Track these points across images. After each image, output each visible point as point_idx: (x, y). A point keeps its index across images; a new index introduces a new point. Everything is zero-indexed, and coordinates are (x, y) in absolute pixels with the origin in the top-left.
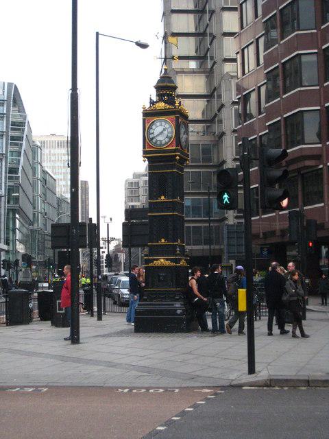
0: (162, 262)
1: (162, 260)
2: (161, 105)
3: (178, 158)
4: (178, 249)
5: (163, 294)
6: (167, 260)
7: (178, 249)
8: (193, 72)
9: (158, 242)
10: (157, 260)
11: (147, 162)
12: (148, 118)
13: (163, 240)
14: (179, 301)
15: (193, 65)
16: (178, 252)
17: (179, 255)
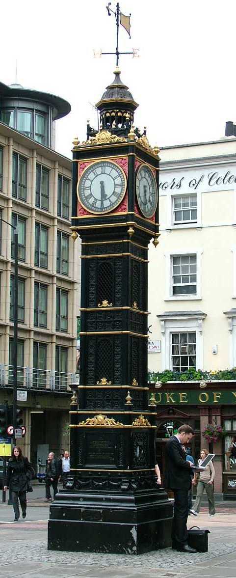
0: (101, 420)
1: (100, 417)
2: (105, 137)
3: (131, 230)
4: (129, 397)
5: (99, 480)
6: (109, 416)
7: (129, 397)
9: (96, 384)
10: (92, 416)
13: (104, 380)
16: (129, 403)
17: (129, 408)
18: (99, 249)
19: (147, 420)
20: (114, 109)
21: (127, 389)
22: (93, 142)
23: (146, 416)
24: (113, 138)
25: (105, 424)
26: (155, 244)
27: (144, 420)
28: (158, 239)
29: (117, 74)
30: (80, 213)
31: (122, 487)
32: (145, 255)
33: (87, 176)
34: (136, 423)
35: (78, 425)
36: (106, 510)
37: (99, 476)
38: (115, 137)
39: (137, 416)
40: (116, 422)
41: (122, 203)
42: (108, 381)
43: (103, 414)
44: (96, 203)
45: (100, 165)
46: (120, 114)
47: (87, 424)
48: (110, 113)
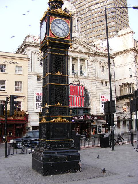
0: (59, 119)
5: (61, 144)
6: (63, 118)
9: (55, 105)
10: (56, 118)
12: (51, 17)
13: (58, 104)
18: (57, 51)
36: (68, 157)
37: (61, 143)
41: (68, 36)
42: (60, 104)
43: (60, 117)
48: (58, 4)
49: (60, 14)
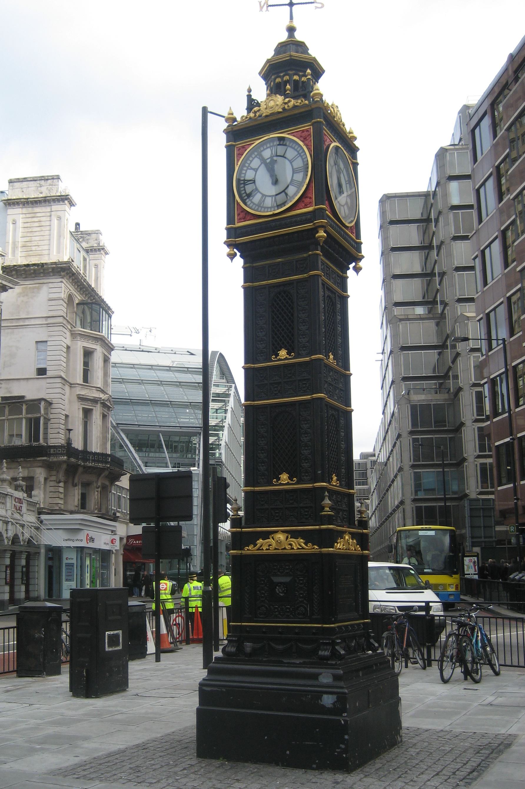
3: (322, 233)
4: (327, 501)
6: (295, 535)
7: (327, 501)
8: (420, 318)
10: (266, 535)
11: (239, 261)
12: (240, 143)
14: (332, 667)
15: (420, 310)
16: (327, 511)
19: (355, 541)
20: (289, 70)
21: (323, 489)
22: (258, 114)
23: (353, 535)
24: (286, 103)
25: (288, 547)
26: (357, 270)
27: (351, 540)
28: (361, 264)
29: (291, 30)
30: (240, 219)
31: (320, 653)
32: (343, 285)
33: (249, 164)
34: (340, 545)
35: (243, 552)
38: (289, 101)
39: (341, 534)
40: (306, 544)
42: (290, 478)
43: (283, 532)
44: (264, 201)
45: (268, 145)
46: (296, 77)
47: (259, 549)
48: (282, 77)
49: (274, 118)
